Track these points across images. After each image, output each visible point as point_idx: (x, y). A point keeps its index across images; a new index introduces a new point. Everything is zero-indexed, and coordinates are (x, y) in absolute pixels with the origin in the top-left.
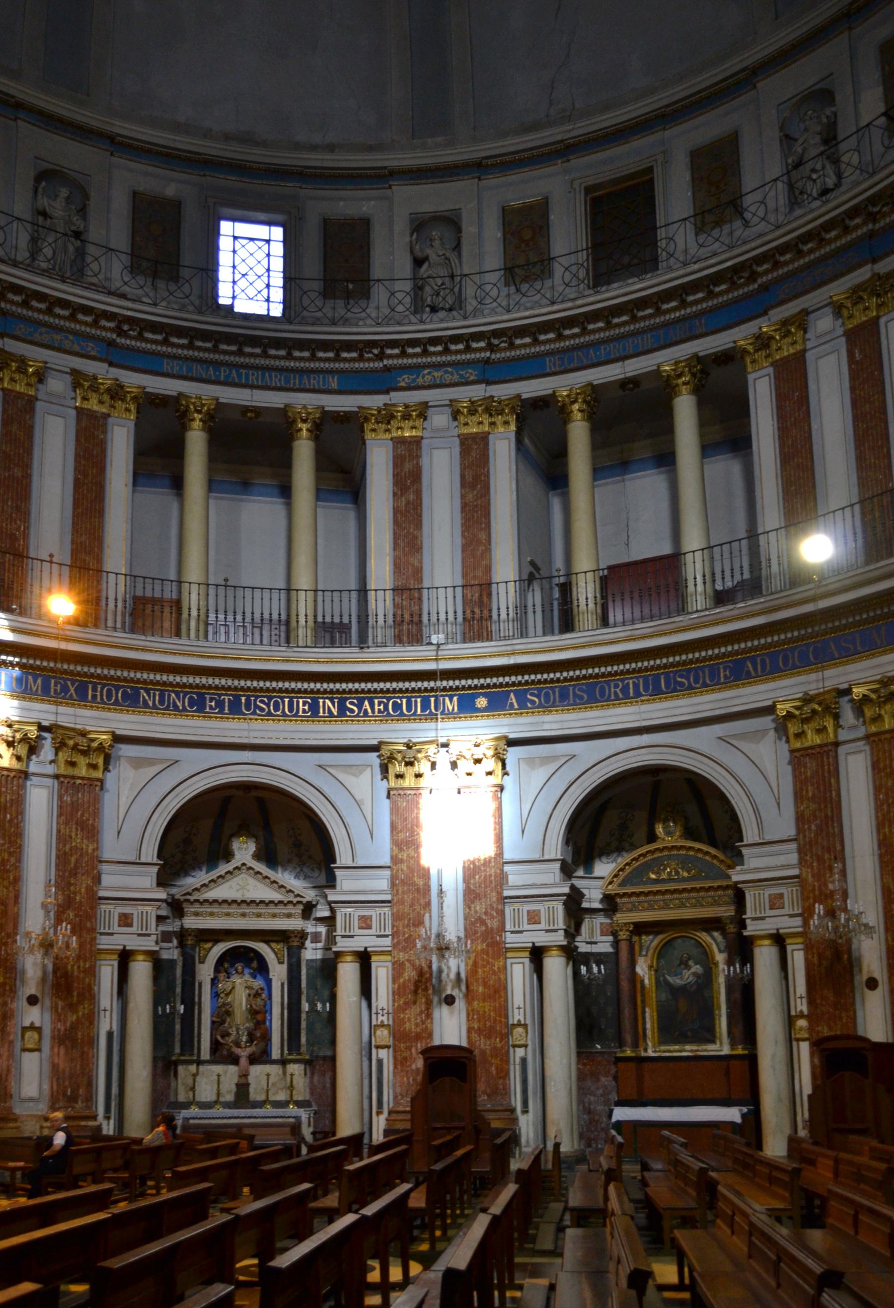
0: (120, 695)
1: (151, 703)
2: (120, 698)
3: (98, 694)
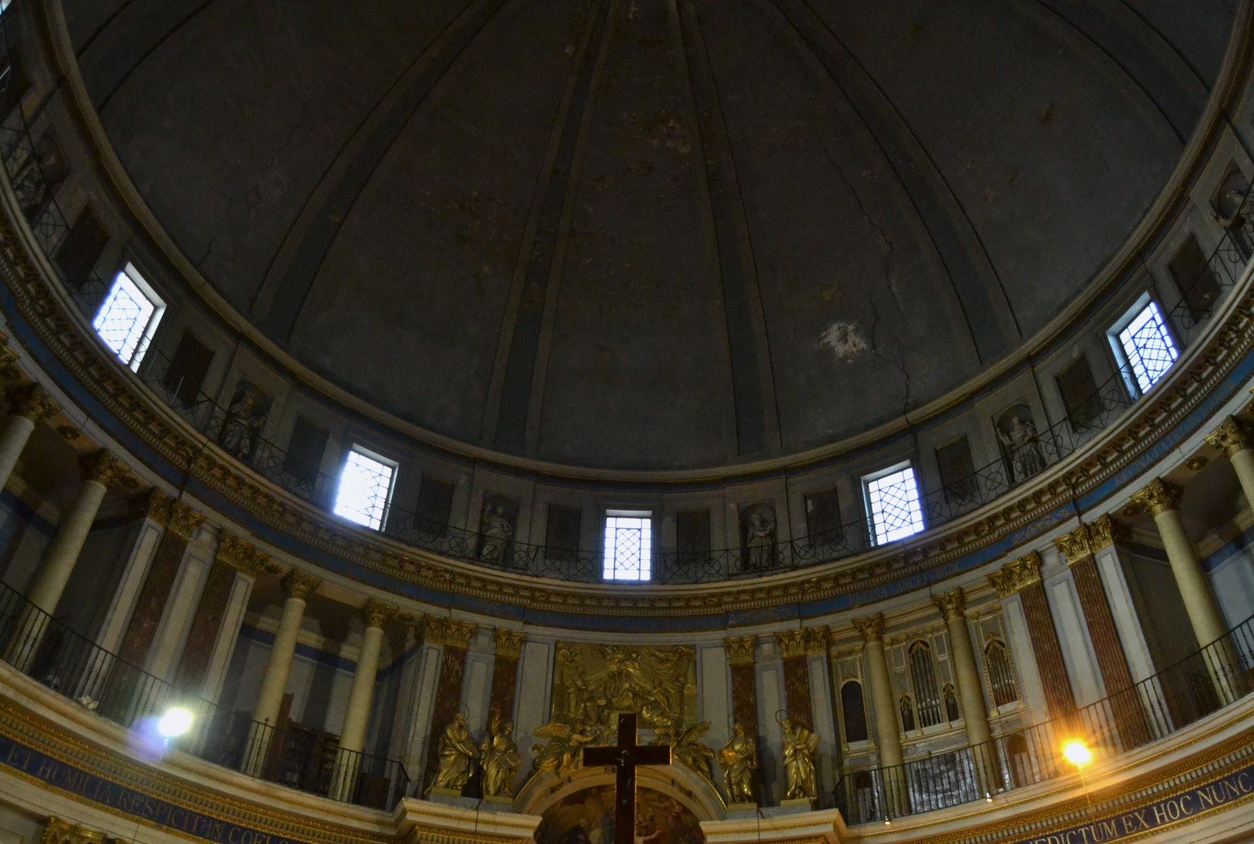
0: (1182, 805)
1: (1210, 801)
2: (1183, 809)
3: (1164, 813)
